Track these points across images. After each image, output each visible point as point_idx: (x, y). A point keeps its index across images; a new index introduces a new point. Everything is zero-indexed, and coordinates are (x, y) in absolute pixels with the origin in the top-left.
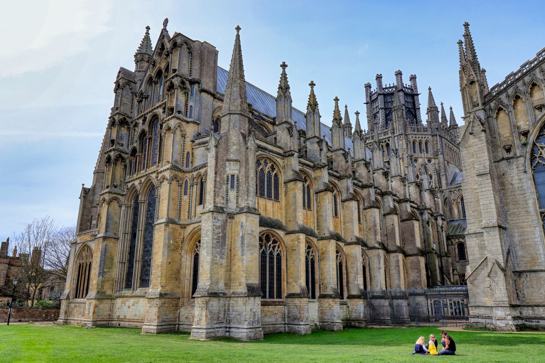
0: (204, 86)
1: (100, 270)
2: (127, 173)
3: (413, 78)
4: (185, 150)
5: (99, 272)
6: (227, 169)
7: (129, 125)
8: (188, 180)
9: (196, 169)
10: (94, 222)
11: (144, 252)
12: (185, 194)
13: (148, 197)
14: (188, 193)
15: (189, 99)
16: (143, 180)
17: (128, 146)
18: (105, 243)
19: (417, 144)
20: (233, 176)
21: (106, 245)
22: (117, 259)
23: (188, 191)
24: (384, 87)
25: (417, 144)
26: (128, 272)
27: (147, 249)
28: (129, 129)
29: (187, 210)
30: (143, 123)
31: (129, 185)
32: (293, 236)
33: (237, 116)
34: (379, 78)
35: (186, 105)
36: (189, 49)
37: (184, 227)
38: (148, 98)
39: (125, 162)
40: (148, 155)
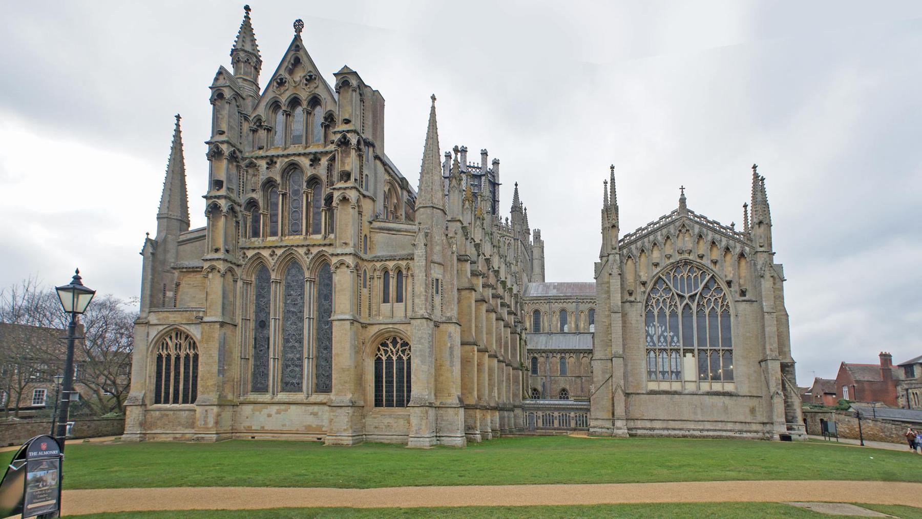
1: (219, 367)
2: (240, 234)
4: (362, 232)
5: (219, 370)
6: (432, 272)
7: (238, 162)
8: (367, 270)
9: (379, 259)
10: (170, 294)
11: (284, 347)
12: (365, 287)
13: (285, 277)
14: (368, 286)
15: (364, 166)
16: (279, 252)
17: (239, 194)
18: (224, 330)
20: (437, 280)
21: (225, 334)
22: (236, 354)
23: (368, 283)
26: (255, 371)
27: (290, 344)
28: (238, 167)
29: (368, 307)
30: (267, 168)
31: (250, 254)
33: (439, 211)
35: (361, 173)
36: (361, 95)
37: (365, 326)
39: (236, 217)
40: (282, 217)
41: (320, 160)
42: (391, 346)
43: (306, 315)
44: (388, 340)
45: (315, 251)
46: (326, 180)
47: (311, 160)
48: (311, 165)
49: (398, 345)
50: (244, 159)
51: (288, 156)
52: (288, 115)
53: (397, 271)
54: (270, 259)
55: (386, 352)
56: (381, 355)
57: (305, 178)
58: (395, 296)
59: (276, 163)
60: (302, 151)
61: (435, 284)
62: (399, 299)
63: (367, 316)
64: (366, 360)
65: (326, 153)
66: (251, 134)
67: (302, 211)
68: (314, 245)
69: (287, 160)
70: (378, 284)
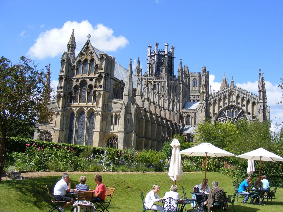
0: (112, 77)
2: (66, 102)
3: (173, 48)
6: (127, 116)
8: (106, 115)
12: (105, 120)
14: (106, 120)
15: (107, 82)
19: (172, 87)
20: (129, 119)
23: (106, 119)
24: (159, 50)
25: (172, 87)
30: (76, 82)
32: (141, 139)
34: (157, 45)
38: (78, 69)
39: (66, 97)
41: (93, 79)
42: (112, 139)
43: (85, 128)
44: (111, 137)
45: (89, 109)
46: (94, 86)
47: (90, 79)
48: (90, 81)
49: (115, 139)
50: (69, 79)
51: (83, 78)
52: (83, 65)
53: (116, 115)
54: (75, 110)
55: (111, 141)
56: (109, 142)
57: (87, 85)
58: (115, 123)
59: (79, 80)
60: (87, 77)
61: (128, 120)
62: (116, 124)
63: (105, 129)
64: (104, 143)
65: (95, 78)
66: (71, 70)
67: (86, 95)
68: (89, 107)
69: (82, 79)
70: (109, 119)
